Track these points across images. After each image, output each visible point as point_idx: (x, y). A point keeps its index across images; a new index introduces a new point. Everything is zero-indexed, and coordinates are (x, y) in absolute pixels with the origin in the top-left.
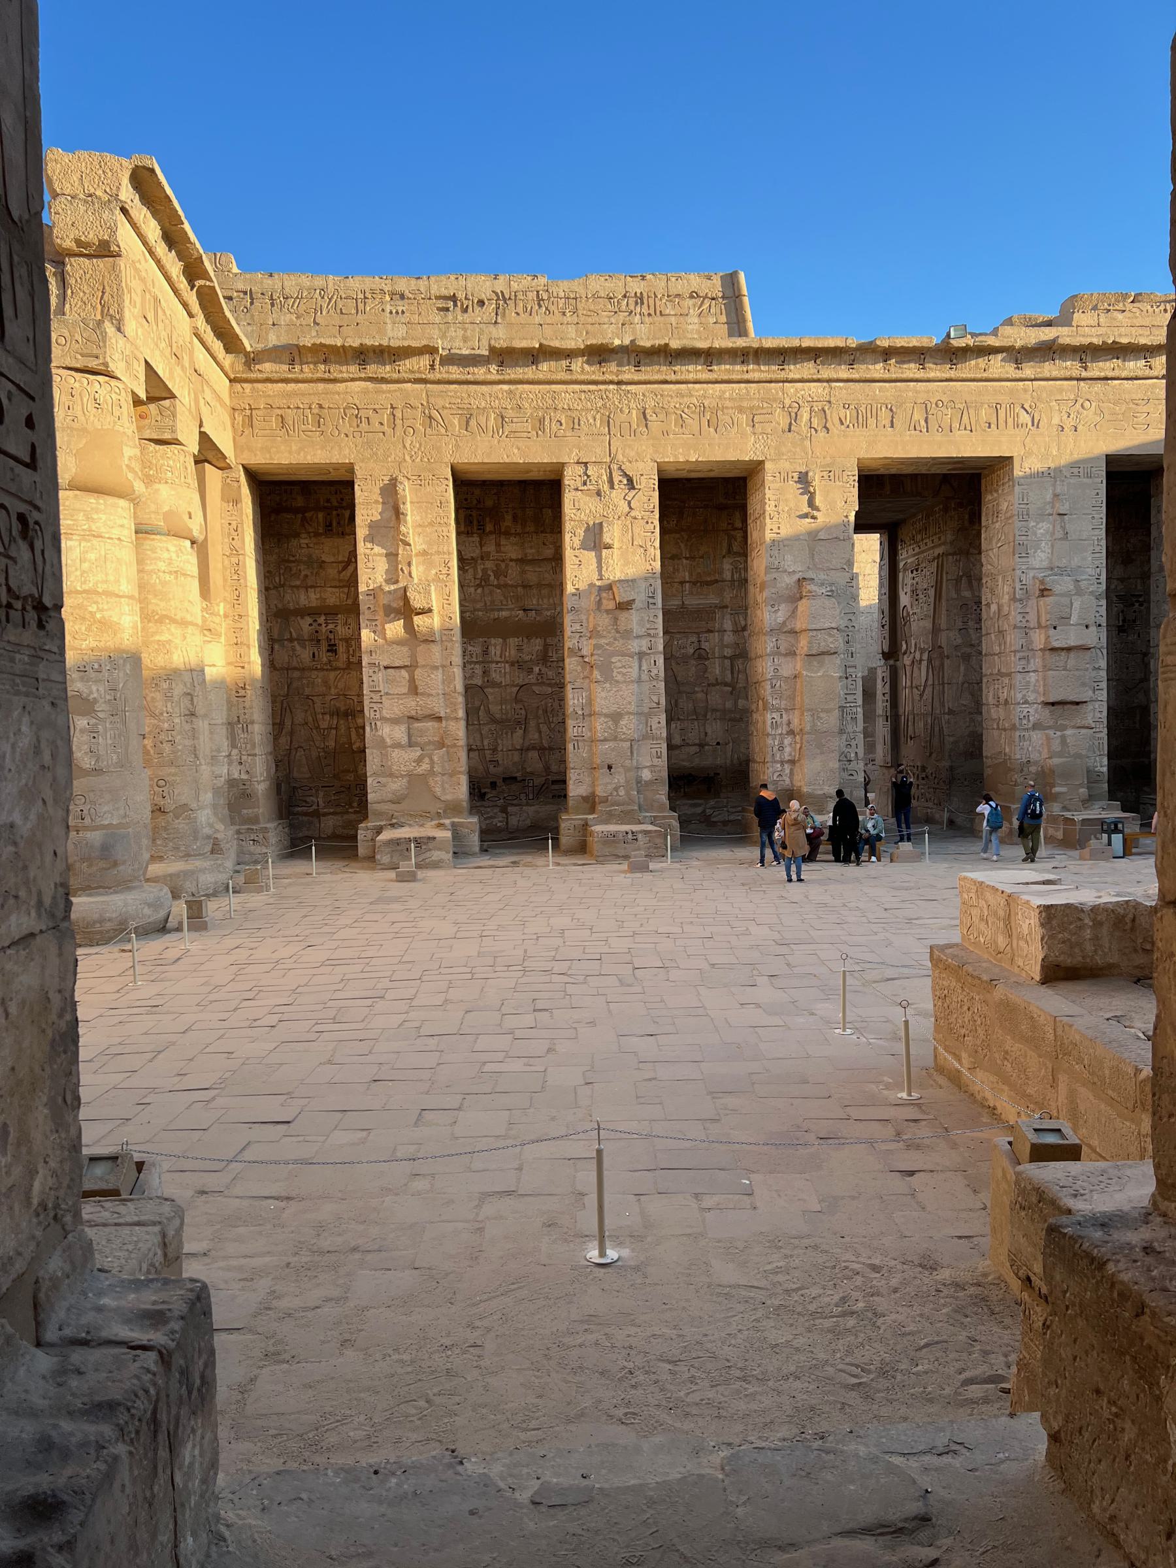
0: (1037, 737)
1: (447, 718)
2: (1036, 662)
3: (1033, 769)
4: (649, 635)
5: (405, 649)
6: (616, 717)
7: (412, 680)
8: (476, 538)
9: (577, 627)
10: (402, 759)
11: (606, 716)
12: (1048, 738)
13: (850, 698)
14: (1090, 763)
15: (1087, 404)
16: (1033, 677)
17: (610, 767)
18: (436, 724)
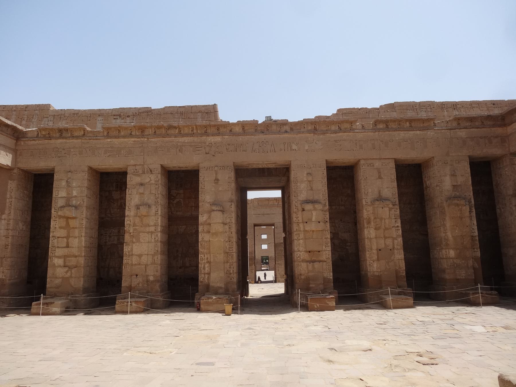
0: (304, 265)
1: (79, 256)
2: (302, 236)
3: (303, 277)
4: (155, 225)
5: (66, 231)
6: (140, 256)
7: (68, 243)
8: (119, 192)
9: (129, 222)
10: (60, 272)
11: (136, 255)
12: (307, 265)
13: (231, 249)
14: (325, 275)
15: (317, 142)
16: (301, 241)
17: (137, 275)
18: (75, 259)
